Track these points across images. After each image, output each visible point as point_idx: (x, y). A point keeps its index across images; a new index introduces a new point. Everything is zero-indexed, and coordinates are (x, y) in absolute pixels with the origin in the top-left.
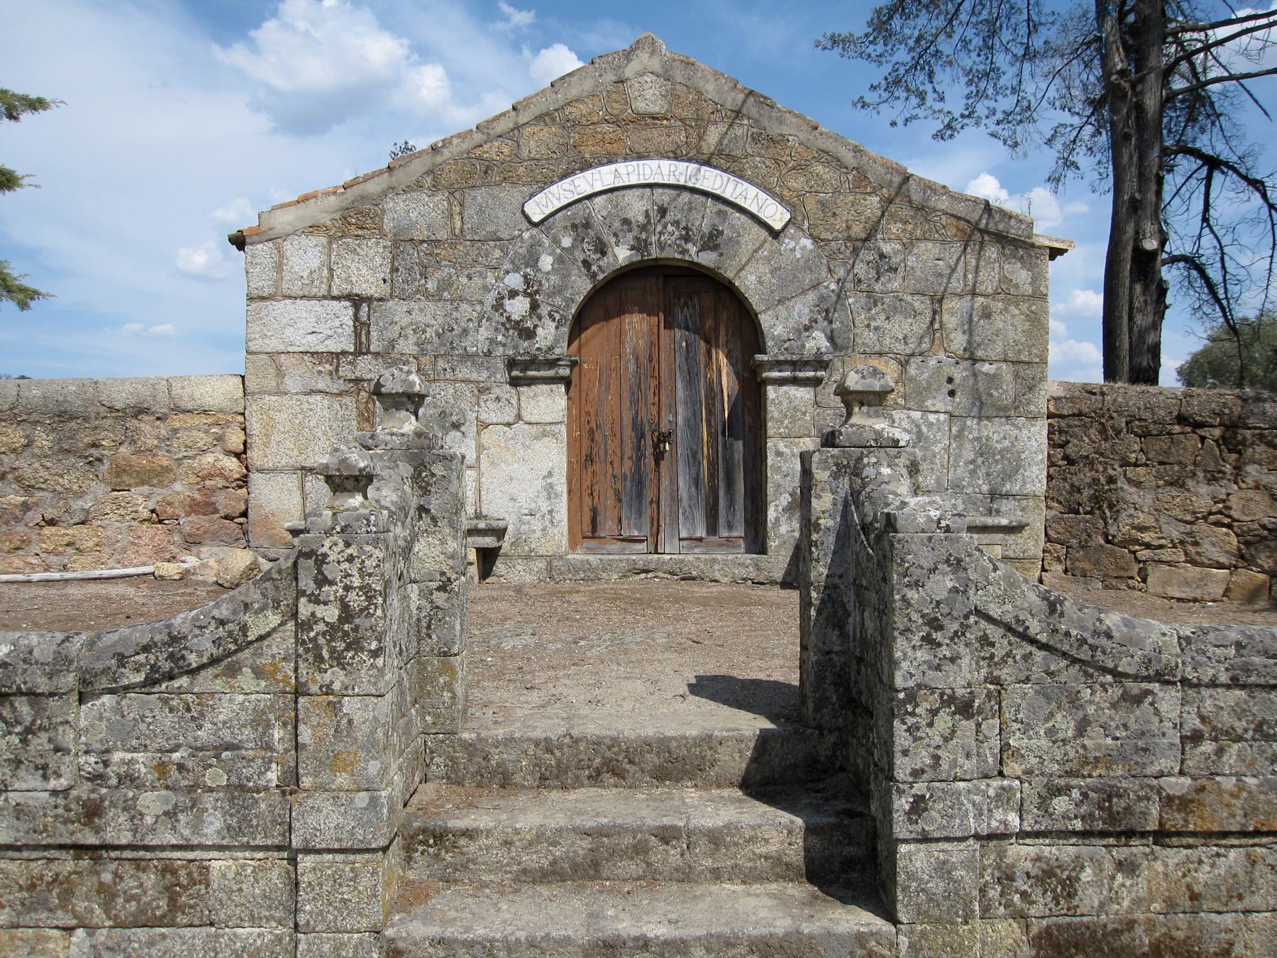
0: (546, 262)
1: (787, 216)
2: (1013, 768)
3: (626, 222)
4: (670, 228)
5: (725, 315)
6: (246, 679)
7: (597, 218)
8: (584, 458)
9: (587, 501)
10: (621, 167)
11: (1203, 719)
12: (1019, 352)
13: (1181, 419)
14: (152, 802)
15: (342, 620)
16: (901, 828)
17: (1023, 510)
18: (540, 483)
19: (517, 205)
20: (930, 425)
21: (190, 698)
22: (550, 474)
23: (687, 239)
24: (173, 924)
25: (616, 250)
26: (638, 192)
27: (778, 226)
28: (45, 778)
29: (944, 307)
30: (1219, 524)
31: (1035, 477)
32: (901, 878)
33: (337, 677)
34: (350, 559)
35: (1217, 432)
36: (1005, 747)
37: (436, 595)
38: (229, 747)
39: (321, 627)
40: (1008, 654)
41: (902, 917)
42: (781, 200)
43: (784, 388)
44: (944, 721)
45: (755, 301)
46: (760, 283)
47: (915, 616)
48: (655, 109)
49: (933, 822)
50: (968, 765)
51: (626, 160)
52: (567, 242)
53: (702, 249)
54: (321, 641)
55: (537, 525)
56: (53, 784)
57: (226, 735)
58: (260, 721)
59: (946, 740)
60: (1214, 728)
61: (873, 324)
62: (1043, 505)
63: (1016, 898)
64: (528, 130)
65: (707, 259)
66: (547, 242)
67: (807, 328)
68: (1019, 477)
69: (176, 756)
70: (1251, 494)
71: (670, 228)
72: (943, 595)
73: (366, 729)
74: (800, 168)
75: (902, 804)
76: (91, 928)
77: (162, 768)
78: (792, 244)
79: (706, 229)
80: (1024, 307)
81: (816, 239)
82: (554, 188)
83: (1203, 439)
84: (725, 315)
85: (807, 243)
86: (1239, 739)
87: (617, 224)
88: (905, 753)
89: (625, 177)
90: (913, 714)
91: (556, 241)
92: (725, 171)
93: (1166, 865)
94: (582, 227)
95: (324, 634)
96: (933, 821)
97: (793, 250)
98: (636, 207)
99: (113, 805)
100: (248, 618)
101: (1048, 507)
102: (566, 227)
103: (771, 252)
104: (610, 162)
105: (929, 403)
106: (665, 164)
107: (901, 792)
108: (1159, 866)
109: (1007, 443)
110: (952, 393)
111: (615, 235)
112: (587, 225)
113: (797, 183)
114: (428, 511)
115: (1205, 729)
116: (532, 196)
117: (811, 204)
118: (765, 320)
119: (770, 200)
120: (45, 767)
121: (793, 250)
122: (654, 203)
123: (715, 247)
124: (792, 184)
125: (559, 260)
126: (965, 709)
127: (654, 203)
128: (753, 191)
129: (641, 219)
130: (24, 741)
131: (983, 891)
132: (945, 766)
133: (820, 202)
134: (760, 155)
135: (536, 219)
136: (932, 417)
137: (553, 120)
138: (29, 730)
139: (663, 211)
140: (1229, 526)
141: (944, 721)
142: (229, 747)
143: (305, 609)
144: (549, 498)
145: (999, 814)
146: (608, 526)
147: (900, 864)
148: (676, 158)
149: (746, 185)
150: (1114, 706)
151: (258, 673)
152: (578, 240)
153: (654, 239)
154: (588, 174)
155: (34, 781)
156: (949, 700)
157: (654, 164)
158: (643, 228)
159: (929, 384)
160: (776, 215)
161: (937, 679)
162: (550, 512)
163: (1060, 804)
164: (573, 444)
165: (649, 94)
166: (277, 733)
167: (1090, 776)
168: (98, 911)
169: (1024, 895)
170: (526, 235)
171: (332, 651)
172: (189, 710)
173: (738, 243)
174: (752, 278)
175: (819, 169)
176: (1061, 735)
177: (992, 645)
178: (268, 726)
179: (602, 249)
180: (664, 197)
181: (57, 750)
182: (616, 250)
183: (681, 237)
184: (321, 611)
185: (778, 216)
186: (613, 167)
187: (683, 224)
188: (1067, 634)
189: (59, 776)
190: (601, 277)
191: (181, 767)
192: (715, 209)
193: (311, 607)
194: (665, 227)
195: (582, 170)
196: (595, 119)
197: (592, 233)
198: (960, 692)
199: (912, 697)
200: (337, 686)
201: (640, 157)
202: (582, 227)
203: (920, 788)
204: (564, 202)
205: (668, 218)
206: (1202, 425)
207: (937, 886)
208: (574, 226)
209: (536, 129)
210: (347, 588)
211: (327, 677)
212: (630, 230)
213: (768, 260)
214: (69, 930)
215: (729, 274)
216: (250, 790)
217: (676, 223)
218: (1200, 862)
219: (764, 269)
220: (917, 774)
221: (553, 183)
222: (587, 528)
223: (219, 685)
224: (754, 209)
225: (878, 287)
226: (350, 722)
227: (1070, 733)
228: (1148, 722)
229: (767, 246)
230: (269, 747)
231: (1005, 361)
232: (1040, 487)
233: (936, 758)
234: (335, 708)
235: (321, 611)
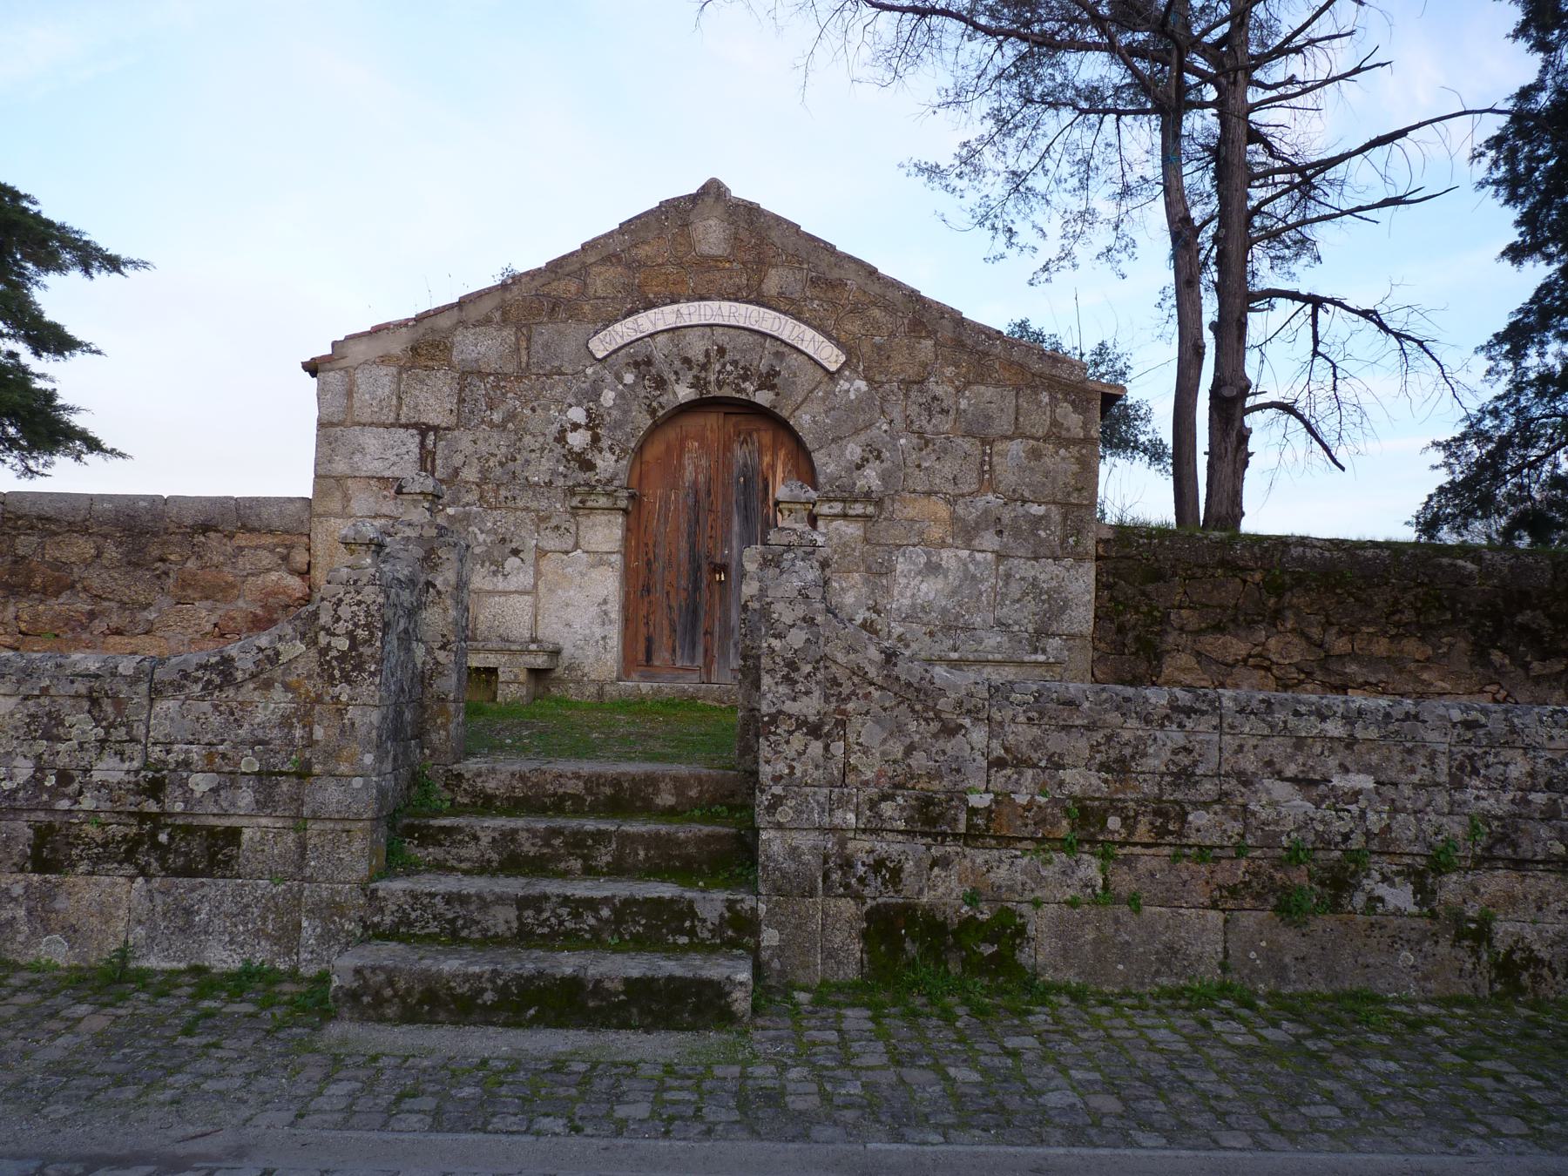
0: (608, 398)
1: (843, 359)
2: (851, 778)
3: (687, 361)
4: (729, 368)
5: (782, 454)
6: (278, 693)
7: (658, 356)
8: (639, 586)
9: (643, 630)
10: (684, 307)
11: (1006, 750)
12: (1069, 494)
13: (1223, 563)
14: (200, 783)
15: (351, 648)
16: (762, 820)
17: (1069, 649)
18: (594, 610)
19: (582, 341)
20: (977, 564)
21: (234, 704)
22: (605, 602)
23: (745, 378)
24: (211, 875)
25: (677, 388)
26: (698, 331)
27: (833, 368)
28: (122, 760)
29: (995, 449)
30: (1256, 667)
31: (1082, 617)
32: (762, 859)
33: (344, 692)
34: (359, 603)
35: (1258, 576)
36: (847, 764)
37: (437, 652)
38: (261, 742)
39: (334, 653)
40: (853, 693)
41: (763, 890)
42: (839, 344)
43: (836, 524)
44: (798, 740)
45: (809, 440)
46: (815, 422)
47: (778, 660)
48: (716, 251)
49: (784, 814)
50: (818, 774)
51: (688, 300)
52: (629, 378)
53: (760, 388)
54: (335, 663)
55: (591, 652)
56: (126, 765)
57: (260, 734)
58: (285, 723)
59: (800, 754)
60: (1015, 758)
61: (925, 464)
62: (1090, 646)
63: (853, 881)
64: (596, 269)
65: (763, 398)
66: (609, 378)
67: (859, 467)
68: (1065, 617)
69: (221, 748)
70: (1290, 637)
71: (729, 368)
72: (801, 645)
73: (364, 730)
74: (856, 310)
75: (764, 799)
76: (148, 877)
77: (210, 757)
78: (846, 386)
79: (763, 369)
80: (1074, 450)
81: (869, 380)
82: (618, 326)
83: (1245, 582)
84: (782, 454)
85: (862, 385)
86: (1035, 766)
87: (677, 364)
88: (768, 762)
89: (755, 314)
90: (775, 734)
91: (619, 378)
92: (785, 313)
93: (973, 862)
94: (642, 364)
95: (336, 658)
96: (787, 814)
97: (848, 391)
98: (697, 348)
99: (172, 783)
100: (280, 647)
101: (1095, 649)
102: (628, 364)
103: (826, 393)
104: (674, 302)
105: (976, 542)
106: (726, 305)
107: (762, 791)
108: (967, 862)
109: (1054, 583)
110: (1000, 533)
111: (676, 373)
112: (649, 362)
113: (853, 326)
114: (434, 586)
115: (1009, 757)
116: (596, 333)
117: (866, 348)
118: (819, 458)
119: (827, 343)
120: (122, 754)
121: (848, 391)
122: (714, 343)
123: (772, 387)
124: (848, 327)
125: (621, 395)
126: (815, 731)
127: (714, 343)
128: (810, 333)
129: (702, 359)
130: (107, 733)
131: (826, 877)
132: (798, 773)
133: (874, 345)
134: (818, 298)
135: (600, 355)
136: (979, 556)
137: (620, 260)
138: (111, 725)
139: (722, 351)
140: (1268, 669)
141: (798, 740)
142: (261, 742)
143: (323, 639)
144: (604, 624)
145: (839, 813)
146: (661, 657)
147: (761, 848)
148: (736, 300)
149: (804, 327)
150: (935, 736)
151: (287, 687)
152: (640, 377)
153: (712, 378)
154: (651, 313)
155: (113, 762)
156: (802, 723)
157: (715, 304)
158: (704, 367)
159: (977, 523)
160: (831, 356)
161: (789, 707)
162: (604, 638)
163: (887, 808)
164: (628, 575)
165: (712, 238)
166: (298, 733)
167: (913, 788)
168: (155, 864)
169: (861, 880)
170: (589, 371)
171: (342, 670)
172: (232, 714)
173: (794, 383)
174: (807, 417)
175: (876, 312)
176: (891, 757)
177: (840, 685)
178: (291, 726)
179: (661, 383)
180: (722, 338)
181: (131, 741)
182: (677, 388)
183: (740, 377)
184: (335, 642)
185: (833, 358)
186: (675, 307)
187: (742, 364)
188: (898, 678)
189: (132, 760)
190: (661, 413)
191: (224, 756)
192: (773, 350)
193: (328, 638)
194: (724, 366)
195: (646, 309)
196: (660, 261)
197: (654, 371)
198: (811, 719)
199: (774, 719)
200: (344, 698)
201: (702, 298)
202: (642, 364)
203: (778, 790)
204: (627, 340)
205: (727, 358)
206: (1244, 569)
207: (789, 866)
208: (637, 365)
209: (603, 269)
210: (356, 625)
211: (337, 689)
212: (690, 369)
213: (824, 399)
214: (132, 879)
215: (785, 414)
216: (275, 774)
217: (735, 363)
218: (1001, 861)
219: (817, 408)
220: (777, 779)
221: (617, 321)
222: (641, 656)
223: (256, 696)
224: (810, 352)
225: (929, 428)
226: (353, 724)
227: (900, 756)
228: (961, 749)
229: (823, 386)
230: (291, 742)
231: (1054, 503)
232: (1087, 627)
233: (792, 768)
234: (340, 713)
235: (335, 642)
